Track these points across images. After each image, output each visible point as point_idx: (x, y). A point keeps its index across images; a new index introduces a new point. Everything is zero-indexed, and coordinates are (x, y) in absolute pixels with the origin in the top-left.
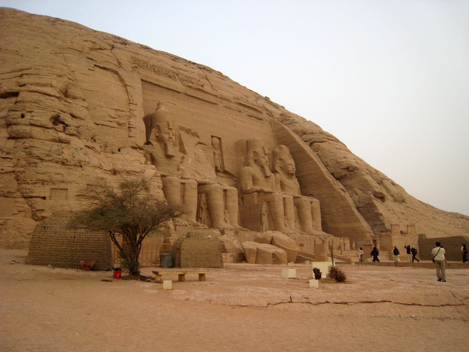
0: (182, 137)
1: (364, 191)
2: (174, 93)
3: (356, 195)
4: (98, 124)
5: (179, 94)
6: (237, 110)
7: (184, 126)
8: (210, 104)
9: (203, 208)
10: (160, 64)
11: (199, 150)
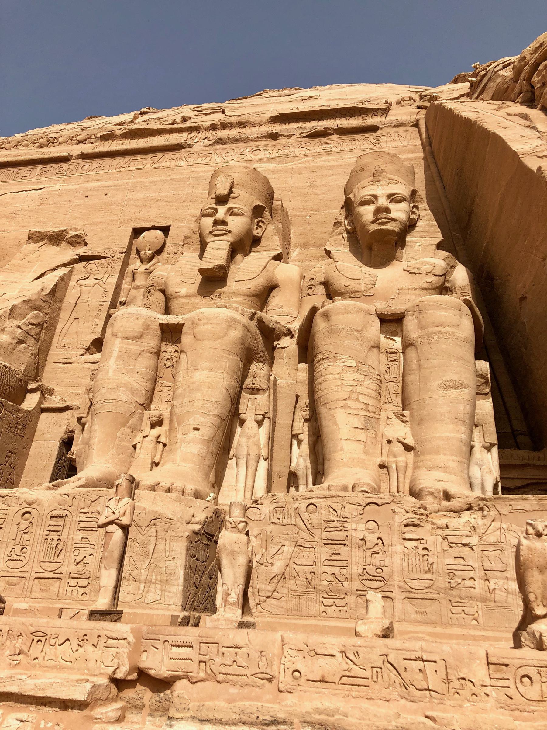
6: (264, 137)
7: (42, 230)
8: (159, 155)
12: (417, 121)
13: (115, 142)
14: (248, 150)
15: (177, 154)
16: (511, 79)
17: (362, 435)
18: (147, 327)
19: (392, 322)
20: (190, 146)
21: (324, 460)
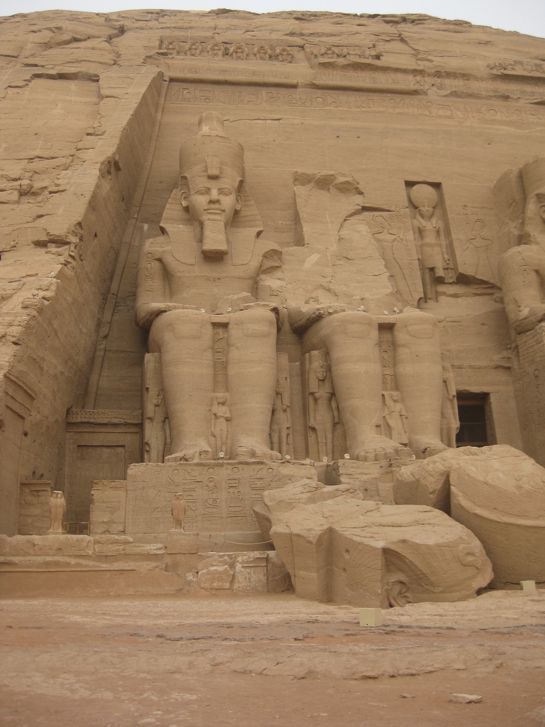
0: (298, 200)
5: (292, 90)
6: (495, 96)
7: (310, 171)
9: (317, 395)
10: (248, 35)
11: (360, 230)
13: (335, 72)
15: (415, 100)
20: (425, 93)
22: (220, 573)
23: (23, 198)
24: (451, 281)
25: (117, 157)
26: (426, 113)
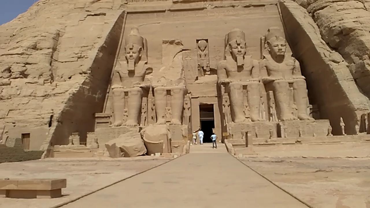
1: (361, 56)
2: (159, 14)
3: (353, 64)
4: (62, 62)
6: (231, 6)
7: (167, 40)
8: (197, 11)
12: (277, 4)
14: (226, 11)
15: (202, 11)
16: (307, 3)
17: (289, 108)
18: (241, 86)
19: (291, 84)
20: (206, 8)
21: (281, 112)
22: (101, 152)
23: (79, 59)
24: (208, 70)
25: (104, 45)
26: (206, 15)
